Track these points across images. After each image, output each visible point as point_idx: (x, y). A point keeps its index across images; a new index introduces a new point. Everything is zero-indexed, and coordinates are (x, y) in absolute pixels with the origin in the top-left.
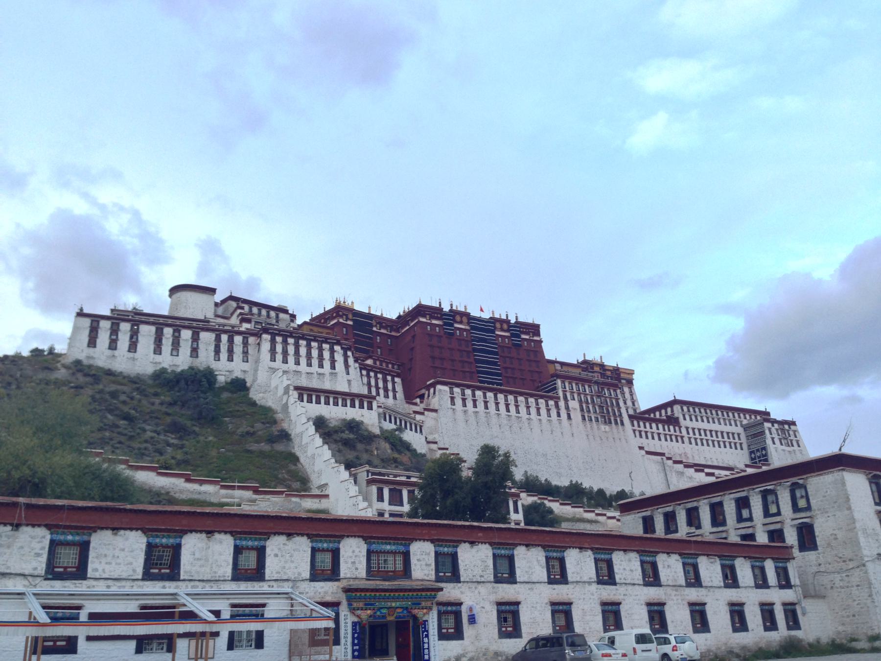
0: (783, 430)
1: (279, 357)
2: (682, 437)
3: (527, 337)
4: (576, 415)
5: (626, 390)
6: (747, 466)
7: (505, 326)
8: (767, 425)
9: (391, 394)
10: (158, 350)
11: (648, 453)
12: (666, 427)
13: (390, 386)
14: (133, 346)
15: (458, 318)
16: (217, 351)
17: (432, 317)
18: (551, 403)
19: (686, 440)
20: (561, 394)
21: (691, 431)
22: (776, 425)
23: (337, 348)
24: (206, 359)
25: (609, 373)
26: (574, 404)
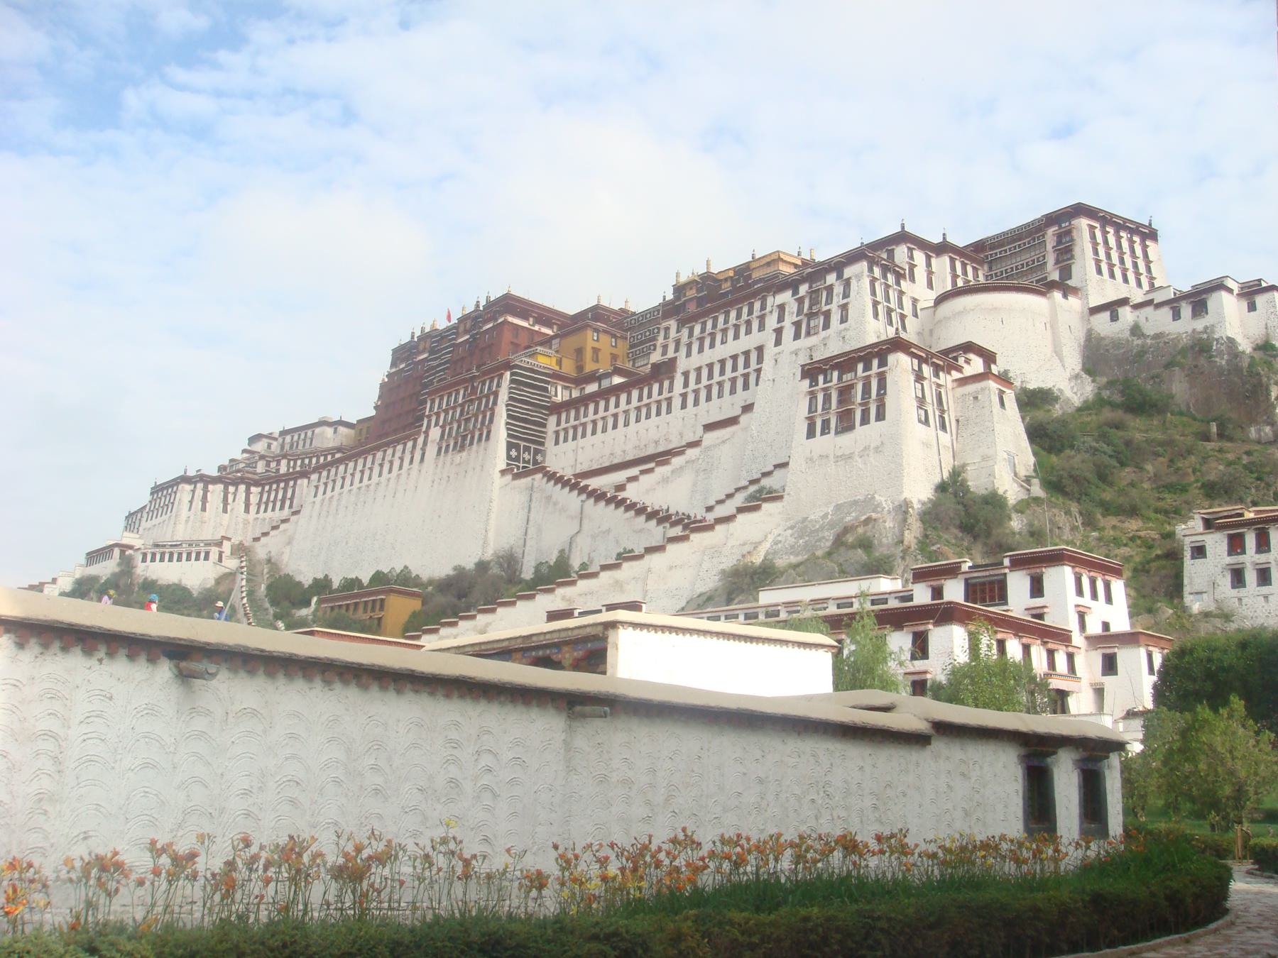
0: (814, 295)
2: (669, 400)
4: (432, 450)
6: (709, 427)
7: (469, 324)
9: (288, 503)
11: (517, 476)
13: (289, 495)
15: (421, 348)
17: (402, 362)
18: (410, 444)
19: (677, 402)
22: (803, 289)
26: (435, 433)
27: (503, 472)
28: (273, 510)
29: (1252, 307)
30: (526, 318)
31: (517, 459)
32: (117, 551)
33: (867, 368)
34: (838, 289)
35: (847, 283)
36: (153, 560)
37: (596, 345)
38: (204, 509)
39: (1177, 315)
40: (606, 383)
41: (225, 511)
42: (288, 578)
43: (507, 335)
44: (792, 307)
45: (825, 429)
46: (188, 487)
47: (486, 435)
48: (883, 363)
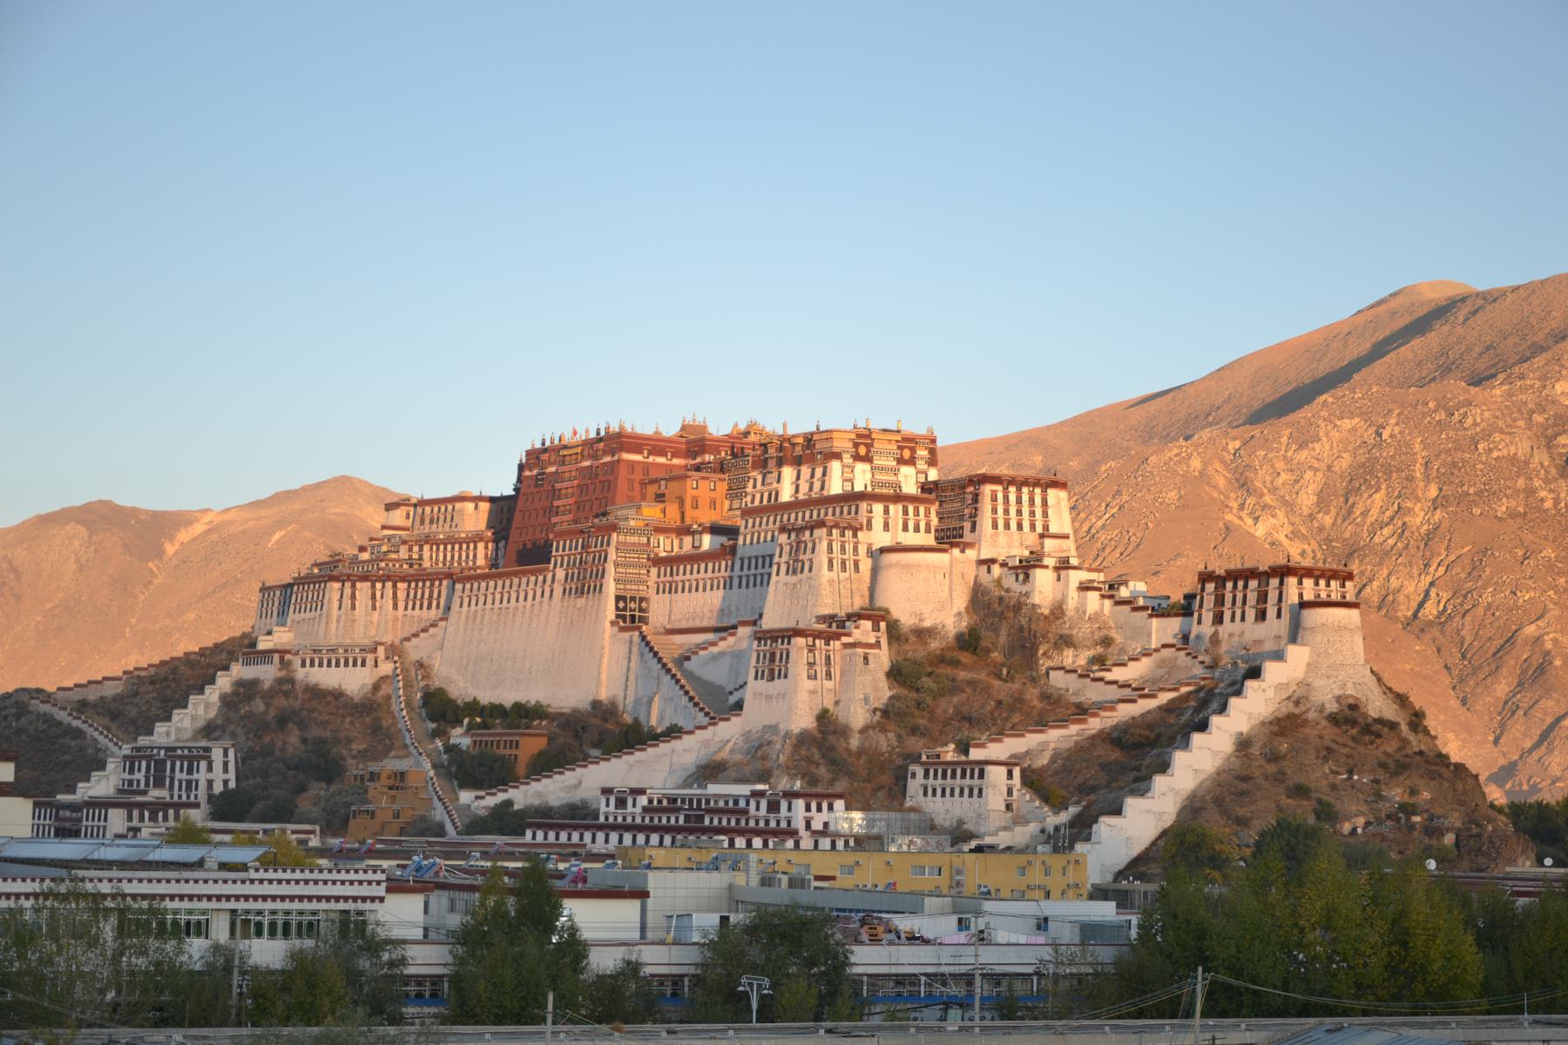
5: (819, 471)
9: (434, 603)
11: (622, 629)
18: (541, 578)
26: (560, 574)
27: (612, 623)
30: (639, 451)
31: (625, 609)
34: (810, 545)
36: (312, 665)
37: (695, 493)
38: (353, 607)
41: (374, 608)
42: (441, 692)
43: (623, 473)
46: (337, 585)
47: (599, 589)
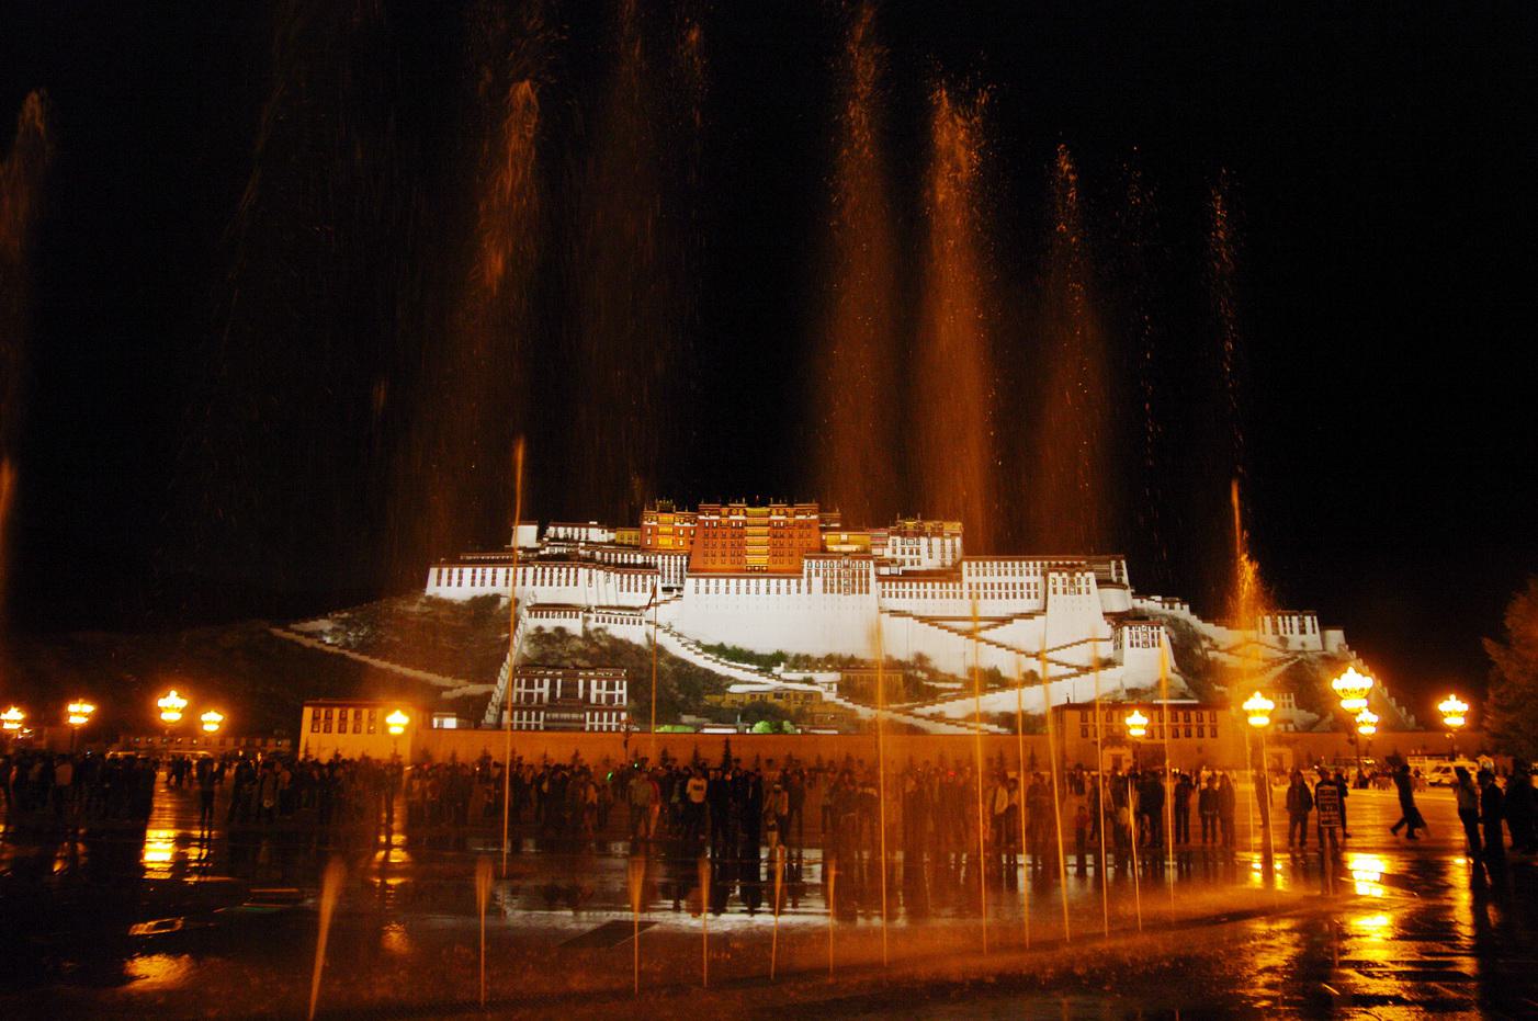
0: (1072, 582)
1: (539, 581)
3: (803, 517)
7: (781, 512)
8: (1052, 575)
10: (473, 584)
12: (944, 585)
14: (460, 584)
15: (734, 511)
16: (507, 578)
17: (710, 514)
19: (966, 595)
20: (805, 571)
21: (974, 586)
22: (1065, 575)
23: (580, 570)
24: (500, 588)
25: (928, 529)
26: (817, 582)
28: (636, 590)
29: (1182, 608)
32: (580, 613)
33: (1152, 628)
34: (1083, 580)
35: (1088, 579)
39: (1163, 607)
40: (894, 570)
44: (1059, 580)
45: (1138, 645)
48: (1158, 629)
